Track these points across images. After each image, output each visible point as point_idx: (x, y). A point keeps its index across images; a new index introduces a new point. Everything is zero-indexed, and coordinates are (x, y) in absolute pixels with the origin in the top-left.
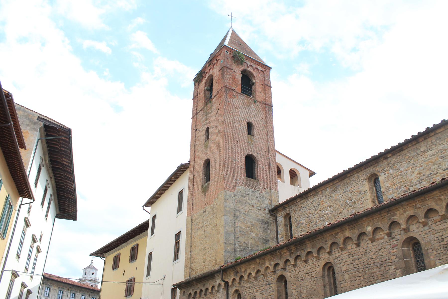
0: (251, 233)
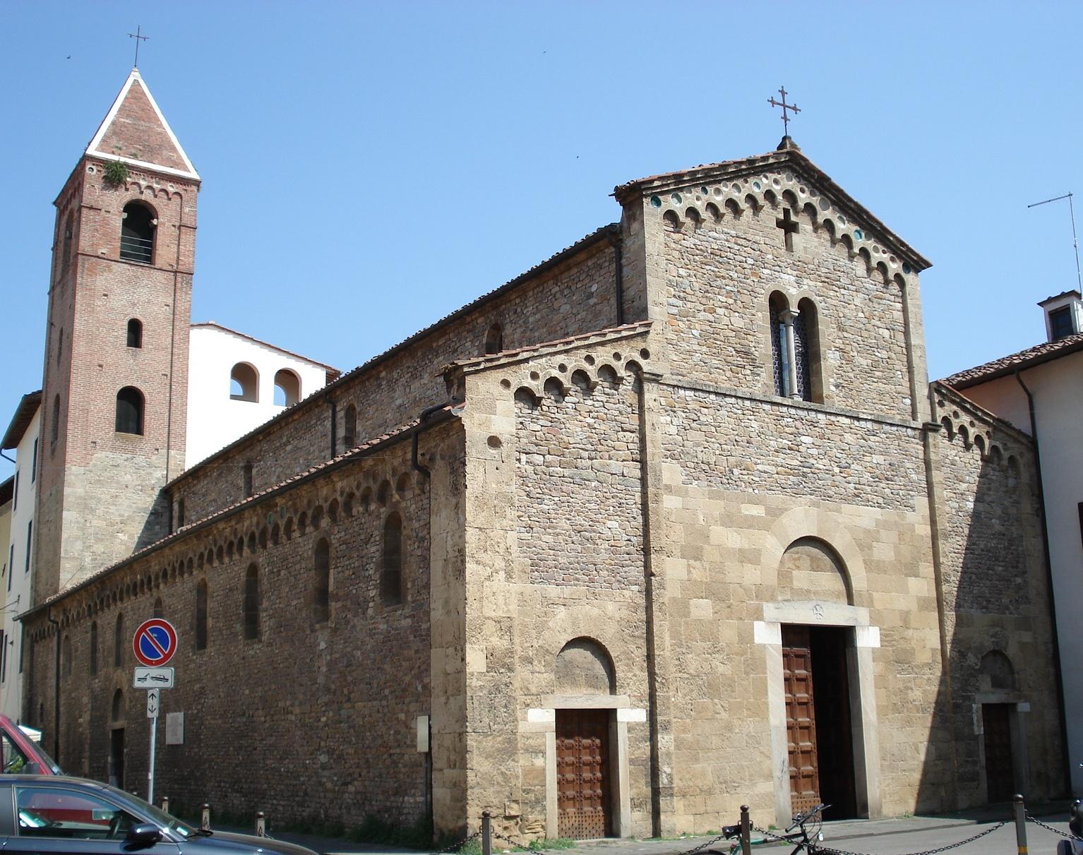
0: (119, 534)
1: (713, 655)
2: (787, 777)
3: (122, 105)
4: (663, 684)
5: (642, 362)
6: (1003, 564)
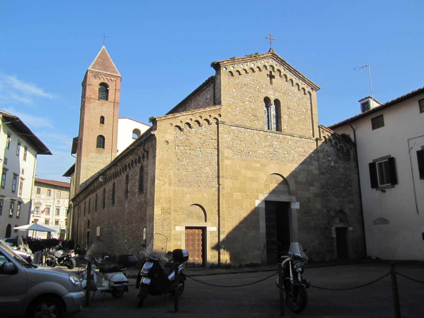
1: (241, 210)
2: (265, 249)
3: (99, 56)
4: (222, 219)
5: (219, 118)
6: (344, 183)
